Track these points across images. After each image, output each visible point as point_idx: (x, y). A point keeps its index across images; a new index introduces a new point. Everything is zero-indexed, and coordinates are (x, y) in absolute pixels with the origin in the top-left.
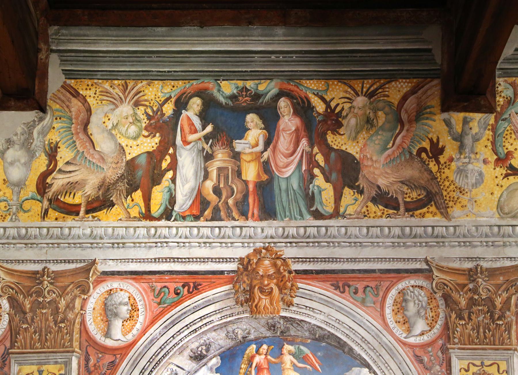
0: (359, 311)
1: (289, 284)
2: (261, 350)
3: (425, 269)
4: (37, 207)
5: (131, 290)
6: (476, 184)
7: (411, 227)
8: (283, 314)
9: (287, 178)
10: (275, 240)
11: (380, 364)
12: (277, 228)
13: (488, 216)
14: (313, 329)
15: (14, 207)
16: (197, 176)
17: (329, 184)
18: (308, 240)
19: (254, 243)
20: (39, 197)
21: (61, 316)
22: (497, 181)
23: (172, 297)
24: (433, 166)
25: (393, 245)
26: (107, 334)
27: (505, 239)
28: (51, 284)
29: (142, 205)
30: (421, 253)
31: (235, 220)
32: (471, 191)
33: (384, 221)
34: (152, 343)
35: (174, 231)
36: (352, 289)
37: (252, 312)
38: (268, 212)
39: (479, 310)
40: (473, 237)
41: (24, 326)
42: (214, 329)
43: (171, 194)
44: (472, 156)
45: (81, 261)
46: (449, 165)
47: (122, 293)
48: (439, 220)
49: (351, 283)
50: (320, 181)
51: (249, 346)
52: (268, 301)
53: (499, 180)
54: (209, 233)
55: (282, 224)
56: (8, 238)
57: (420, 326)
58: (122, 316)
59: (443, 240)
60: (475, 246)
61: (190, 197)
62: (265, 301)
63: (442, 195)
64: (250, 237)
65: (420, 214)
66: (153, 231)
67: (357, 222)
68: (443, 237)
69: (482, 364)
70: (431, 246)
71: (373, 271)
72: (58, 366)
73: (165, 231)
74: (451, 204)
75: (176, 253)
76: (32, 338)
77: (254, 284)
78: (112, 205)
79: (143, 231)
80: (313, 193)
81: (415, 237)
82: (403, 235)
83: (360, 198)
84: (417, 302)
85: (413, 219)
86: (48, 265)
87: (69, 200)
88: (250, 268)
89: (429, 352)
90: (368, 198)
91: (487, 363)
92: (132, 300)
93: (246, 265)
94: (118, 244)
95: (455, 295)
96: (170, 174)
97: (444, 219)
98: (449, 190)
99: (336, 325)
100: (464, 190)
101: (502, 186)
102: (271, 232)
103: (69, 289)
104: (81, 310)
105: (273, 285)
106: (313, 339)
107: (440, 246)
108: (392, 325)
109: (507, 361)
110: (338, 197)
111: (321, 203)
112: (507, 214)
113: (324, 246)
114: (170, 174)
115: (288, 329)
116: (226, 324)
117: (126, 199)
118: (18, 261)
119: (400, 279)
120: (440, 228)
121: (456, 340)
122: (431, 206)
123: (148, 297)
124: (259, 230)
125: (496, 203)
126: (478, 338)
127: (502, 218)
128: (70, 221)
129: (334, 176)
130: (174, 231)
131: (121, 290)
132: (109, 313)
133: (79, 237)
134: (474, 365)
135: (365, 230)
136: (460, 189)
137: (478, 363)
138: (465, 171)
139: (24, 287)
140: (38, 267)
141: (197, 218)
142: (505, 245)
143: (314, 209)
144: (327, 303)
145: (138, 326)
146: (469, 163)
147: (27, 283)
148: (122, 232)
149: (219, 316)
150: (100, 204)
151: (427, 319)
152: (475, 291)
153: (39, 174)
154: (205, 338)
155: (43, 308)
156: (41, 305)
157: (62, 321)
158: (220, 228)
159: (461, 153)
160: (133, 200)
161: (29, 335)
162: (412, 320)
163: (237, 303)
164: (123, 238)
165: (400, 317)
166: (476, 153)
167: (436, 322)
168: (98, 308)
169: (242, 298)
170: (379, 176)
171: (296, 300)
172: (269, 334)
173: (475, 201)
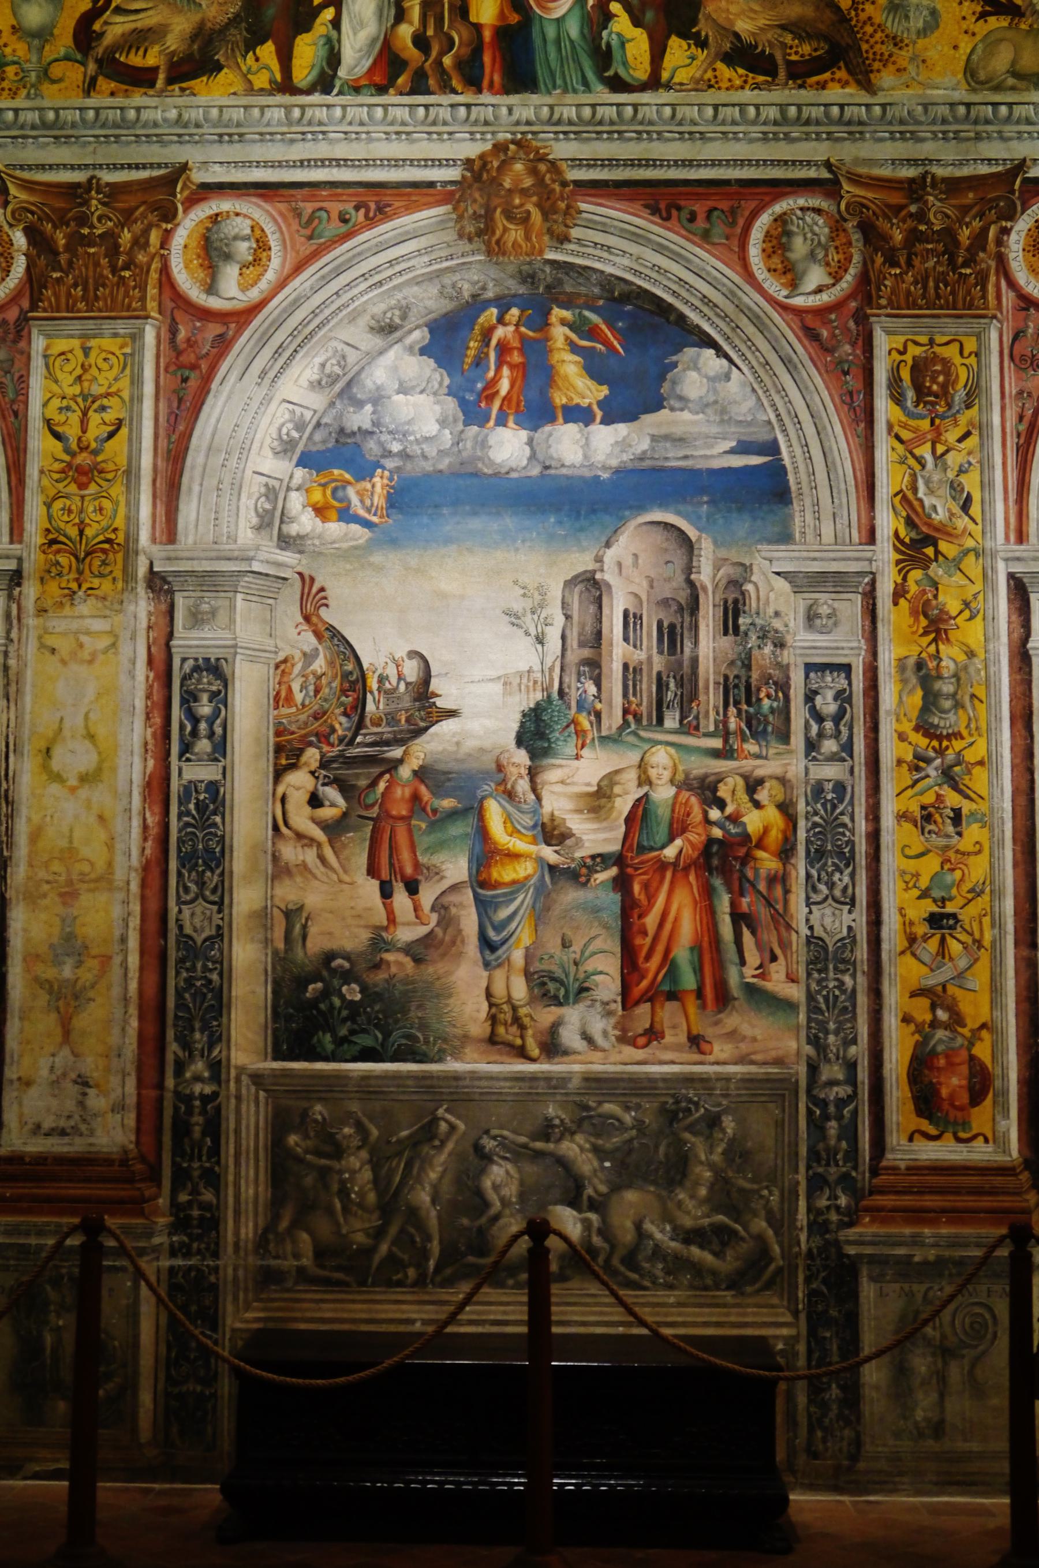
0: (697, 250)
1: (562, 205)
2: (507, 317)
4: (75, 74)
5: (257, 214)
7: (799, 107)
8: (550, 256)
9: (558, 20)
10: (535, 128)
11: (737, 342)
12: (538, 107)
13: (947, 87)
14: (609, 282)
15: (33, 74)
16: (381, 16)
17: (639, 30)
18: (599, 128)
19: (493, 133)
20: (79, 57)
21: (122, 260)
23: (336, 228)
25: (765, 138)
26: (211, 289)
27: (979, 128)
28: (104, 204)
29: (275, 66)
30: (821, 151)
31: (456, 93)
33: (747, 95)
34: (296, 304)
35: (338, 112)
36: (685, 214)
37: (489, 253)
38: (520, 78)
40: (918, 123)
41: (55, 275)
42: (417, 281)
43: (332, 49)
45: (159, 166)
47: (239, 219)
48: (851, 93)
49: (682, 203)
50: (622, 23)
51: (484, 310)
52: (521, 233)
53: (970, 24)
54: (407, 117)
55: (549, 100)
56: (22, 127)
57: (816, 276)
58: (239, 258)
60: (922, 140)
61: (369, 53)
62: (515, 234)
64: (486, 123)
66: (296, 113)
67: (694, 97)
68: (861, 123)
69: (931, 342)
70: (838, 140)
71: (726, 182)
72: (119, 340)
73: (321, 114)
74: (876, 65)
75: (341, 151)
76: (69, 295)
77: (493, 204)
78: (218, 68)
79: (278, 114)
80: (609, 45)
81: (808, 122)
82: (784, 120)
83: (702, 55)
85: (803, 92)
86: (99, 173)
87: (135, 60)
88: (485, 176)
90: (717, 55)
91: (940, 339)
92: (258, 232)
93: (477, 171)
94: (230, 135)
95: (882, 224)
96: (329, 13)
99: (654, 275)
102: (528, 113)
103: (137, 213)
104: (162, 247)
105: (530, 207)
106: (607, 299)
107: (855, 140)
108: (760, 271)
109: (978, 336)
110: (658, 54)
111: (625, 63)
112: (982, 83)
113: (631, 139)
114: (329, 13)
115: (560, 282)
116: (439, 274)
117: (244, 57)
118: (41, 167)
119: (776, 198)
120: (856, 109)
121: (883, 302)
123: (289, 226)
124: (504, 110)
125: (963, 64)
126: (924, 297)
127: (974, 90)
128: (138, 99)
129: (649, 16)
130: (338, 112)
131: (237, 214)
132: (214, 254)
133: (156, 125)
135: (709, 112)
137: (923, 339)
139: (53, 210)
140: (78, 177)
141: (382, 90)
142: (978, 137)
143: (610, 73)
144: (635, 238)
145: (270, 275)
147: (60, 204)
148: (238, 114)
149: (426, 259)
150: (195, 64)
151: (828, 264)
152: (921, 216)
153: (77, 15)
154: (399, 296)
155: (90, 246)
156: (88, 241)
157: (126, 267)
158: (427, 107)
160: (257, 60)
161: (63, 289)
162: (800, 267)
163: (461, 236)
164: (239, 125)
165: (776, 262)
168: (193, 244)
169: (470, 229)
170: (737, 15)
171: (575, 233)
172: (522, 290)
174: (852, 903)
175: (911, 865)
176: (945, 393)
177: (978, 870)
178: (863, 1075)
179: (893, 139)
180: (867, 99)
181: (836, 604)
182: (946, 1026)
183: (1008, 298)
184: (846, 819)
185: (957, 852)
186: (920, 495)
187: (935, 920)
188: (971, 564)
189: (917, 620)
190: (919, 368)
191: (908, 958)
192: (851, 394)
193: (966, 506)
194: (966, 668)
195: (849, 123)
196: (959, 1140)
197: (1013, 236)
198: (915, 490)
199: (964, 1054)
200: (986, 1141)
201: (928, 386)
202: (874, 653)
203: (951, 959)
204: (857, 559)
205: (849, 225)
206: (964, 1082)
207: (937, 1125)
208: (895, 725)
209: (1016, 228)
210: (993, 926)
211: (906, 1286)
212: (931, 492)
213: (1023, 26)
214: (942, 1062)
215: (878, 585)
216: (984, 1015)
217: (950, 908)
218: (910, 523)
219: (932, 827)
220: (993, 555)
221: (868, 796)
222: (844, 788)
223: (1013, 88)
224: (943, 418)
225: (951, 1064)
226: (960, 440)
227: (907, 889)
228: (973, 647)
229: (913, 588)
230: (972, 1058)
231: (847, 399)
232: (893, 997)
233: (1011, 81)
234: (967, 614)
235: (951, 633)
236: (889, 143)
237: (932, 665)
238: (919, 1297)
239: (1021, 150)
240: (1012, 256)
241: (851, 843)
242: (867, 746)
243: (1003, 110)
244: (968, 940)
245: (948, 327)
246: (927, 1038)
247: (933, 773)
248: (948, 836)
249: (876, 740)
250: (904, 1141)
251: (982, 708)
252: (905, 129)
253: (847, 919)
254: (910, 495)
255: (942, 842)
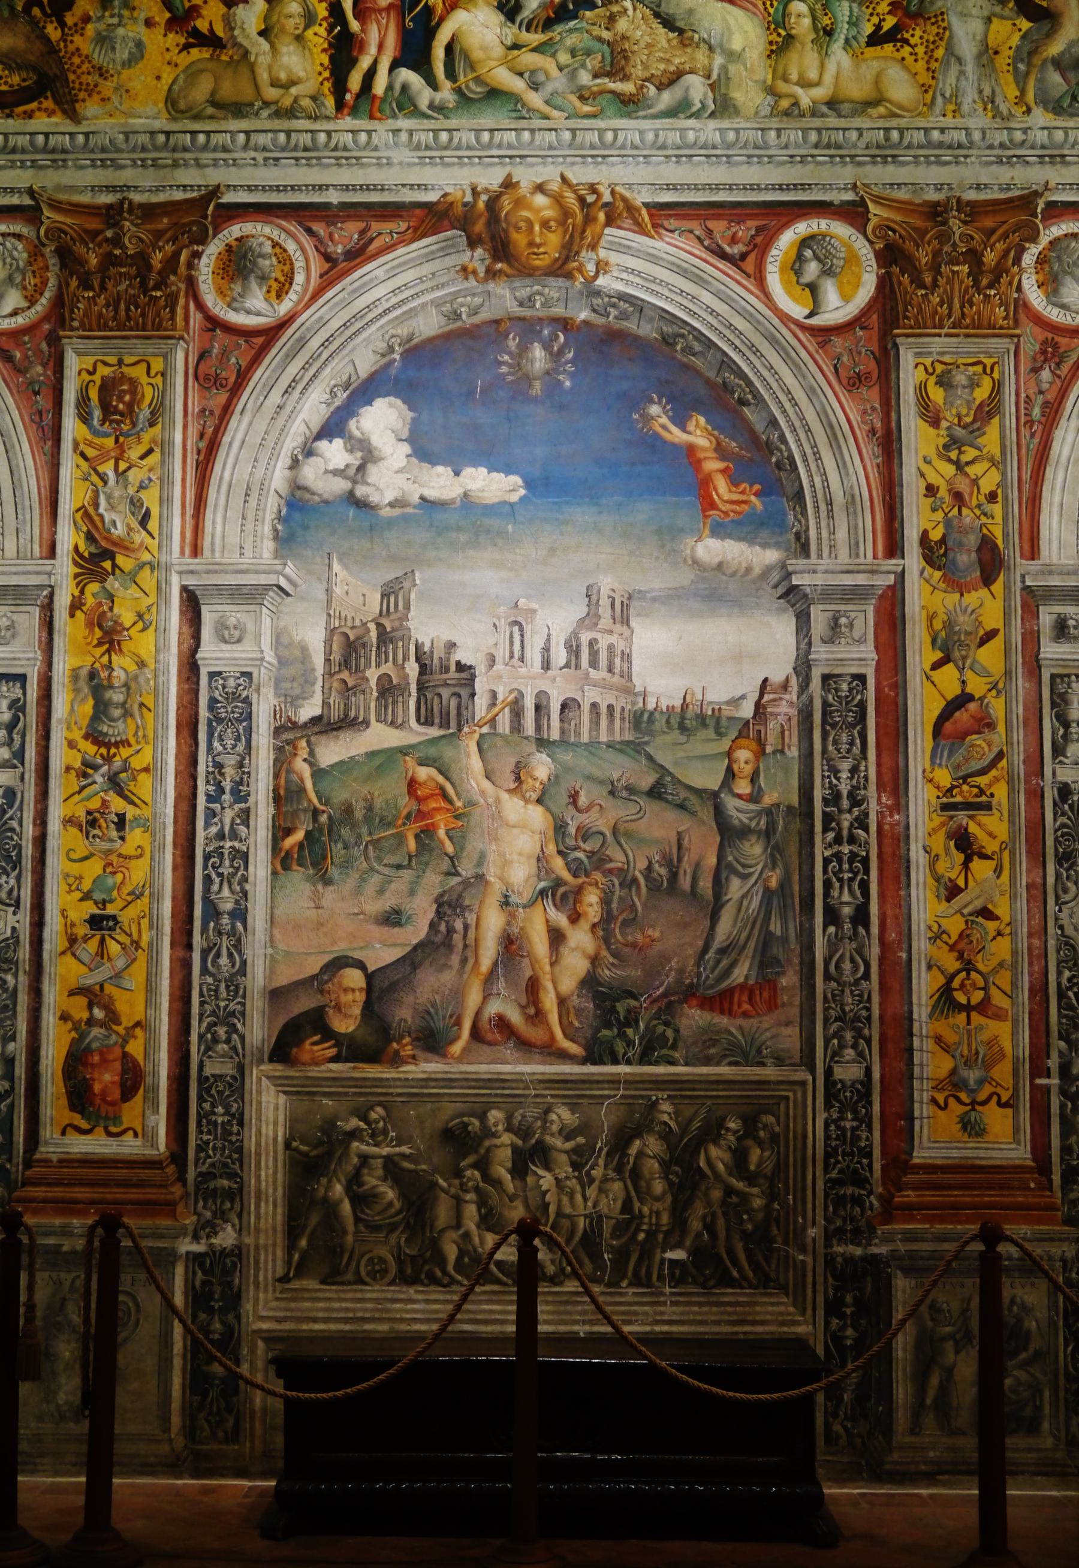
3: (29, 206)
6: (130, 61)
13: (149, 116)
22: (168, 57)
24: (53, 31)
27: (177, 155)
30: (23, 178)
32: (119, 73)
39: (121, 274)
40: (119, 150)
44: (126, 13)
46: (83, 29)
48: (57, 122)
53: (173, 55)
59: (63, 156)
63: (67, 79)
65: (25, 112)
68: (64, 151)
69: (120, 362)
70: (41, 167)
74: (82, 95)
81: (13, 151)
84: (8, 260)
85: (10, 121)
89: (25, 343)
91: (128, 360)
95: (79, 249)
97: (68, 121)
98: (79, 71)
100: (107, 72)
101: (176, 65)
107: (57, 168)
109: (165, 357)
112: (182, 112)
120: (60, 138)
121: (76, 324)
122: (46, 98)
125: (164, 94)
126: (114, 319)
127: (174, 119)
134: (105, 364)
136: (100, 69)
137: (112, 360)
138: (111, 39)
142: (175, 165)
146: (119, 25)
151: (25, 288)
152: (116, 241)
159: (104, 8)
166: (134, 9)
167: (41, 294)
173: (127, 91)
174: (17, 905)
175: (75, 868)
176: (130, 412)
177: (138, 872)
178: (20, 1071)
179: (94, 166)
180: (72, 128)
181: (15, 617)
182: (102, 1024)
183: (196, 319)
184: (14, 824)
185: (120, 855)
186: (101, 510)
187: (95, 922)
188: (147, 578)
189: (92, 631)
190: (107, 388)
191: (69, 958)
192: (40, 413)
193: (144, 522)
194: (136, 678)
195: (53, 151)
196: (110, 1134)
197: (204, 260)
198: (96, 505)
199: (118, 1052)
200: (136, 1135)
201: (116, 405)
202: (49, 664)
203: (109, 959)
204: (38, 573)
205: (47, 251)
206: (117, 1078)
207: (88, 1120)
208: (65, 733)
209: (208, 252)
210: (151, 927)
211: (54, 1275)
212: (112, 507)
213: (224, 58)
214: (96, 1058)
215: (56, 598)
216: (139, 1016)
217: (110, 910)
218: (90, 538)
219: (97, 832)
220: (168, 568)
221: (36, 802)
222: (14, 794)
223: (212, 117)
224: (127, 435)
225: (105, 1061)
226: (142, 458)
227: (70, 891)
228: (144, 656)
229: (90, 601)
230: (125, 1055)
231: (37, 418)
232: (53, 995)
233: (210, 110)
234: (140, 625)
235: (125, 646)
236: (90, 170)
237: (104, 675)
238: (67, 1284)
239: (215, 176)
240: (201, 278)
241: (19, 847)
242: (38, 753)
243: (202, 138)
244: (128, 941)
245: (136, 348)
246: (82, 1036)
247: (99, 779)
248: (112, 841)
249: (47, 748)
250: (57, 1135)
251: (149, 716)
252: (105, 156)
253: (11, 920)
254: (91, 510)
255: (105, 846)
